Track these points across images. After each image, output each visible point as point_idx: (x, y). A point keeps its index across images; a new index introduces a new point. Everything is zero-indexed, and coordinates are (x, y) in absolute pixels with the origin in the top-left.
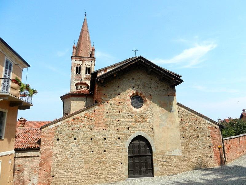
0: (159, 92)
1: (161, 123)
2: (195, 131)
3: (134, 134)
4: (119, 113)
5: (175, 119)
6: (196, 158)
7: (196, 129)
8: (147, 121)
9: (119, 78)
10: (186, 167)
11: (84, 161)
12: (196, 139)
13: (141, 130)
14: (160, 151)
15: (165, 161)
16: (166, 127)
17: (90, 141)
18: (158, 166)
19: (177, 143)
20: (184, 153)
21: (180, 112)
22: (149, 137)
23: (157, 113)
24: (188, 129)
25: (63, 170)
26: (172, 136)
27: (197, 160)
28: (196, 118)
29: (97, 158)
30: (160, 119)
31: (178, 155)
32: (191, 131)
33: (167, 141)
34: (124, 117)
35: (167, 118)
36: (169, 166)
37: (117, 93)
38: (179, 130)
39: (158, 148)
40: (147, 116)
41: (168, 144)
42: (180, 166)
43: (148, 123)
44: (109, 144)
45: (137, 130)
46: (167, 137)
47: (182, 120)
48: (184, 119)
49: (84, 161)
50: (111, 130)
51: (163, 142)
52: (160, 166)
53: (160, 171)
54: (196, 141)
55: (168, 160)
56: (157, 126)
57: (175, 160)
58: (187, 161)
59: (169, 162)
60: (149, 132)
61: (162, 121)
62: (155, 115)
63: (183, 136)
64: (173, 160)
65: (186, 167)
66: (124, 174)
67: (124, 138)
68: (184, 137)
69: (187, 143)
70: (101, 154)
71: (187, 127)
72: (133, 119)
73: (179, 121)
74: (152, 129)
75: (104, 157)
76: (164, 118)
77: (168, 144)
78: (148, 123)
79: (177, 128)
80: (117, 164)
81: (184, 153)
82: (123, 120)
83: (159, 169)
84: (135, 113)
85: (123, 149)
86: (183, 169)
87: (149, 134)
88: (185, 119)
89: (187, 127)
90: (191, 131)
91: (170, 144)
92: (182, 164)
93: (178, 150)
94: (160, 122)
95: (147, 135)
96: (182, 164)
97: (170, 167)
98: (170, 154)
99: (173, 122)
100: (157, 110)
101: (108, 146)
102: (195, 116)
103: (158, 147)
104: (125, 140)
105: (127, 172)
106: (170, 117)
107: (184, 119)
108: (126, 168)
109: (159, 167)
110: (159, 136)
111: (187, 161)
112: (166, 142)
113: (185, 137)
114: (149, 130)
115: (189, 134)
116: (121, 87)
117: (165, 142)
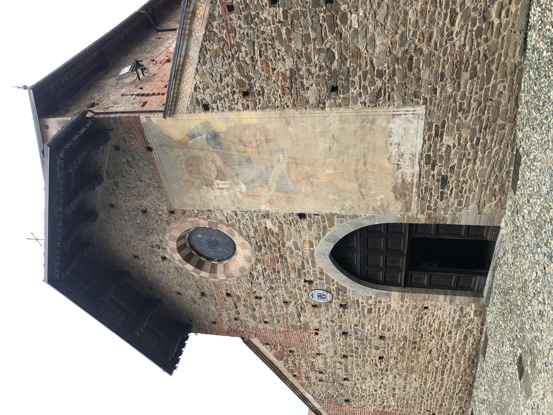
0: (148, 186)
1: (273, 185)
2: (296, 16)
3: (324, 271)
4: (260, 298)
5: (248, 126)
6: (454, 14)
7: (285, 13)
8: (276, 230)
9: (151, 288)
10: (495, 86)
11: (405, 374)
12: (344, 18)
13: (312, 253)
14: (396, 198)
15: (444, 181)
16: (289, 169)
17: (352, 360)
18: (460, 210)
19: (362, 127)
20: (416, 95)
21: (208, 99)
22: (334, 228)
23: (236, 196)
24: (289, 63)
25: (422, 402)
26: (330, 148)
27: (466, 17)
28: (219, 10)
29: (402, 354)
30: (260, 189)
31: (422, 123)
32: (296, 45)
33: (353, 167)
34: (271, 288)
35: (249, 160)
36: (470, 166)
37: (200, 298)
38: (297, 113)
39: (382, 205)
40: (256, 231)
41: (365, 164)
42: (485, 118)
43: (281, 228)
44: (360, 328)
45: (314, 263)
46: (335, 169)
47: (245, 94)
48: (240, 83)
49: (405, 374)
50: (318, 320)
51: (355, 186)
52: (460, 203)
53: (480, 206)
54: (353, 19)
55: (440, 169)
56: (289, 200)
57: (448, 140)
58: (466, 75)
59: (452, 168)
60: (314, 227)
61: (266, 182)
62: (248, 204)
63: (324, 89)
64: (444, 149)
65: (495, 86)
66: (464, 307)
67: (342, 295)
68: (334, 89)
69: (365, 74)
70: (390, 345)
71: (280, 66)
72: (274, 269)
73: (254, 109)
74: (302, 216)
75: (401, 341)
76: (250, 173)
77: (365, 164)
78: (281, 228)
79: (288, 123)
80: (425, 317)
81: (416, 95)
82: (282, 291)
83: (473, 206)
84: (253, 262)
85: (380, 302)
86: (504, 101)
87: (325, 228)
88: (236, 74)
89: (280, 66)
90: (296, 45)
91: (365, 155)
92: (474, 105)
93: (396, 125)
94: (270, 190)
95: (328, 233)
96: (474, 105)
97: (478, 163)
98: (412, 161)
99: (263, 139)
100: (223, 196)
101: (368, 330)
102: (211, 17)
103: (379, 204)
104: (350, 294)
105: (459, 299)
106: (242, 148)
107: (240, 83)
108: (445, 301)
109: (467, 205)
110: (331, 197)
111: (466, 75)
112: (356, 171)
113: (331, 83)
114: (310, 227)
115: (315, 59)
116: (177, 288)
117: (357, 179)
